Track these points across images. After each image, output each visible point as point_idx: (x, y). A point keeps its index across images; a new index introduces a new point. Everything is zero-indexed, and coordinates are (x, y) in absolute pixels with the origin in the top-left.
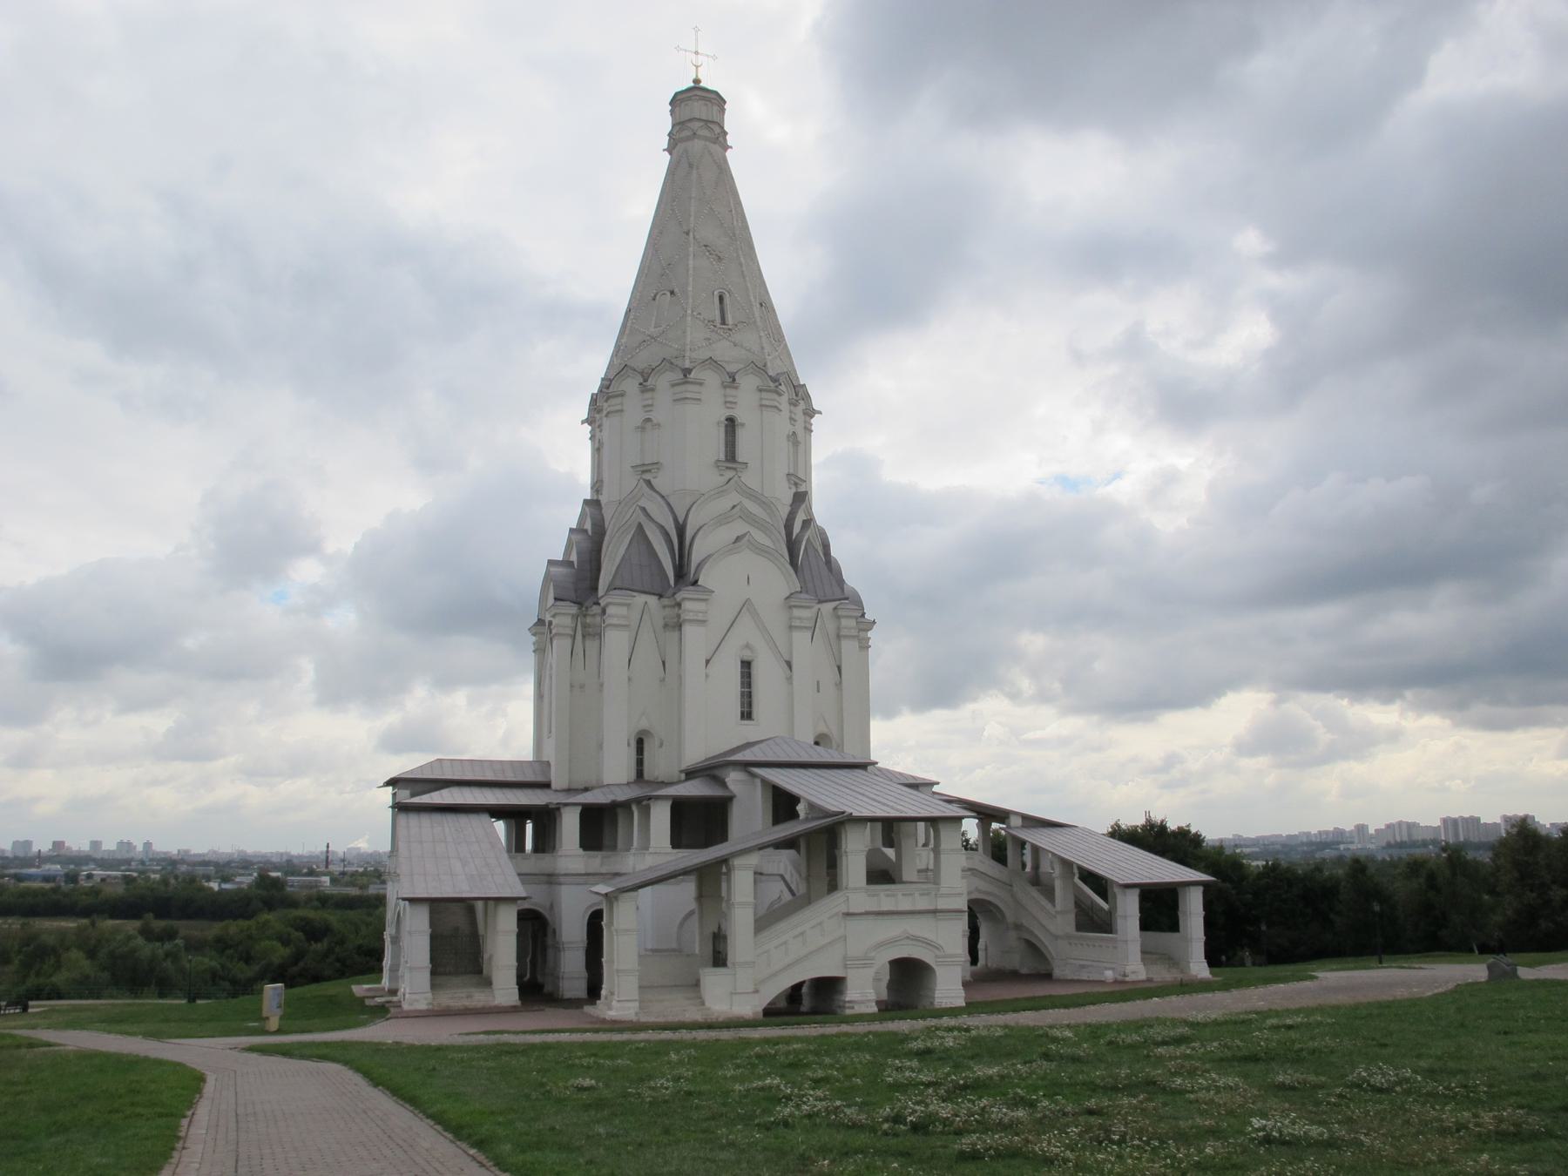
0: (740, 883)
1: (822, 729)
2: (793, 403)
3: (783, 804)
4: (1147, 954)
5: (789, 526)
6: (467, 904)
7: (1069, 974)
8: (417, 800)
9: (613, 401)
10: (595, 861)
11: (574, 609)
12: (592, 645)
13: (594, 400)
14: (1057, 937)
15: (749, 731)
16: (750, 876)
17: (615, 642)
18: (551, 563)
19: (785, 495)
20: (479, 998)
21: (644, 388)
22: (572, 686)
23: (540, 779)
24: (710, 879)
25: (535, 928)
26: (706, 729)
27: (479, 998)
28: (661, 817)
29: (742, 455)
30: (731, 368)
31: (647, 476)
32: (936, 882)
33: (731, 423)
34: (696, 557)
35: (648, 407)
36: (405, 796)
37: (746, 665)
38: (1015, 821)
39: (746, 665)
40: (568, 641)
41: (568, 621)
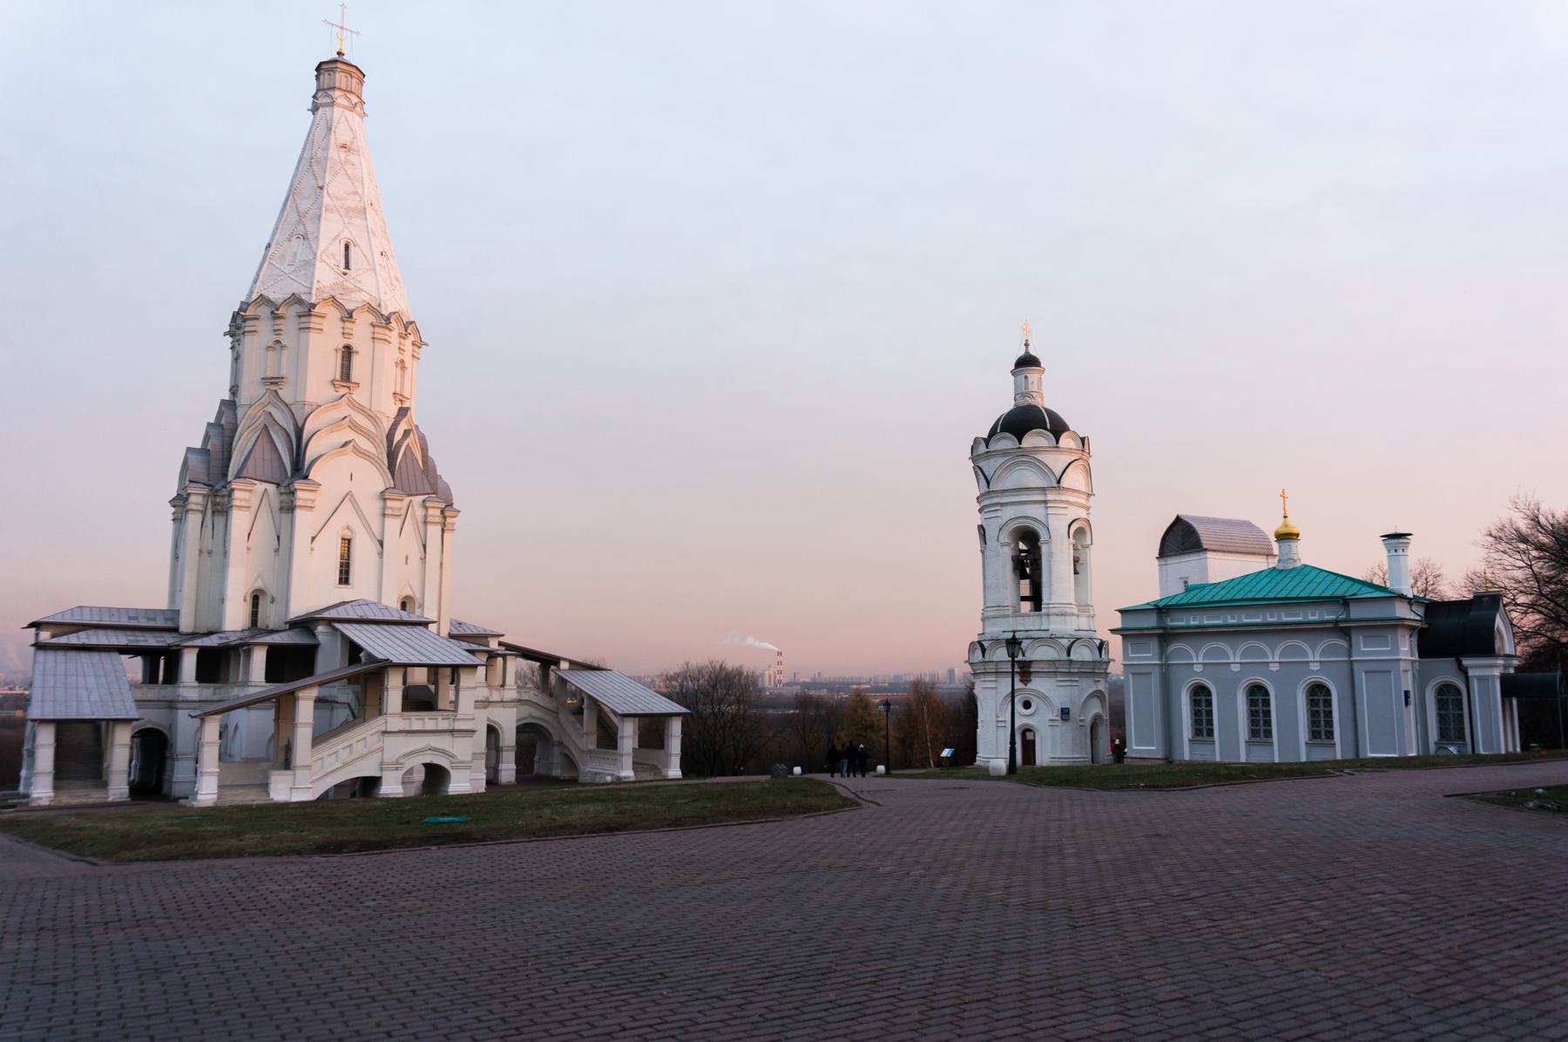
0: (305, 709)
1: (408, 592)
2: (403, 337)
3: (354, 651)
4: (636, 765)
5: (390, 436)
6: (95, 724)
7: (588, 779)
8: (55, 641)
9: (249, 323)
10: (208, 691)
11: (205, 491)
12: (220, 520)
13: (235, 316)
14: (582, 752)
15: (346, 593)
16: (311, 704)
17: (239, 520)
18: (189, 449)
19: (392, 411)
20: (95, 796)
21: (275, 316)
22: (201, 551)
23: (170, 624)
24: (284, 706)
25: (155, 748)
26: (311, 590)
27: (95, 796)
28: (259, 658)
29: (354, 378)
30: (349, 307)
31: (274, 387)
32: (456, 711)
33: (348, 352)
34: (310, 454)
36: (45, 636)
37: (347, 542)
38: (564, 665)
39: (347, 542)
40: (200, 516)
41: (199, 499)
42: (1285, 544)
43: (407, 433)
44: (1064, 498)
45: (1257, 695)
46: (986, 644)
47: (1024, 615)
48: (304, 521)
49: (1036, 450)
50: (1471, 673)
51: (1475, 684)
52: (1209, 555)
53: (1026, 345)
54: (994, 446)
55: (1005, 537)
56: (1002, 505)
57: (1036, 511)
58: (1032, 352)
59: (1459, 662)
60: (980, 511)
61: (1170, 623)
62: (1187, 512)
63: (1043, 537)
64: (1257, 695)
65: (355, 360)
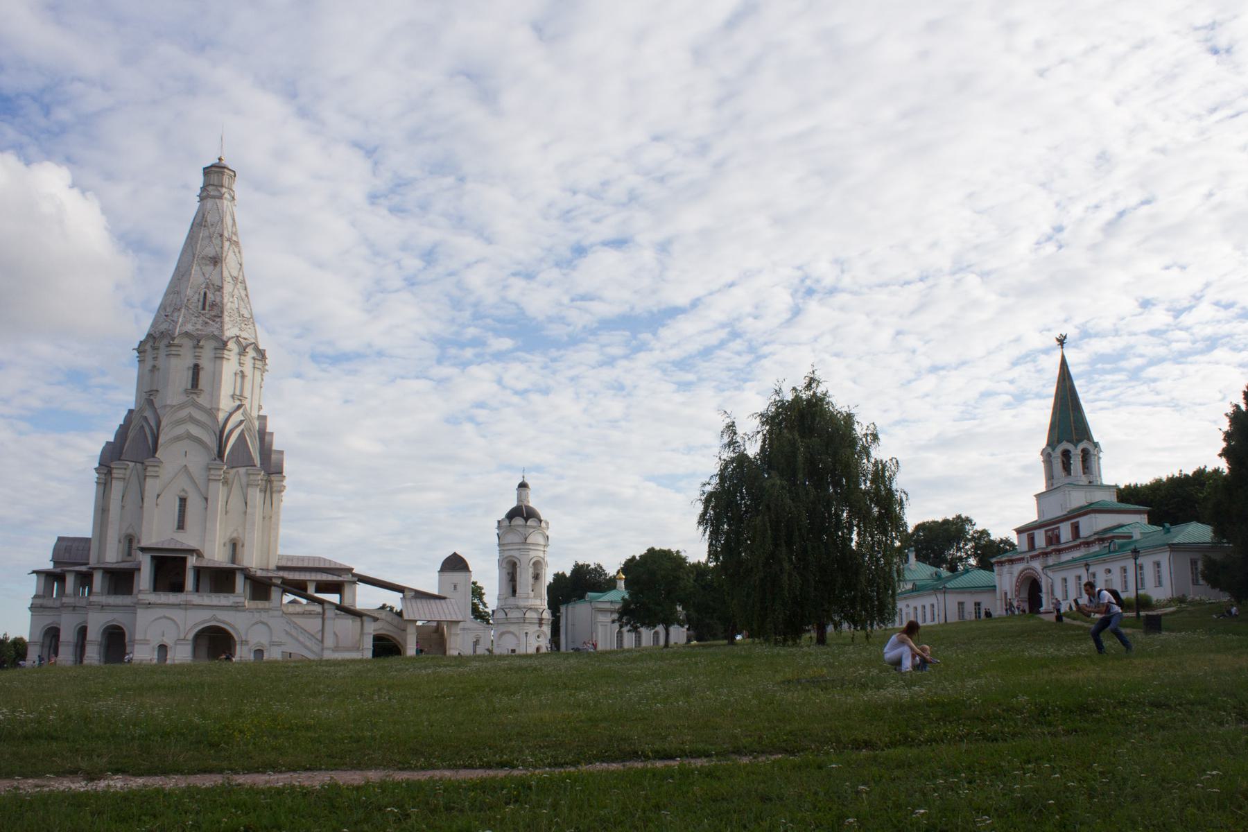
17: (117, 487)
33: (196, 369)
34: (161, 441)
35: (155, 359)
37: (183, 501)
39: (183, 501)
43: (241, 422)
48: (151, 486)
65: (202, 375)
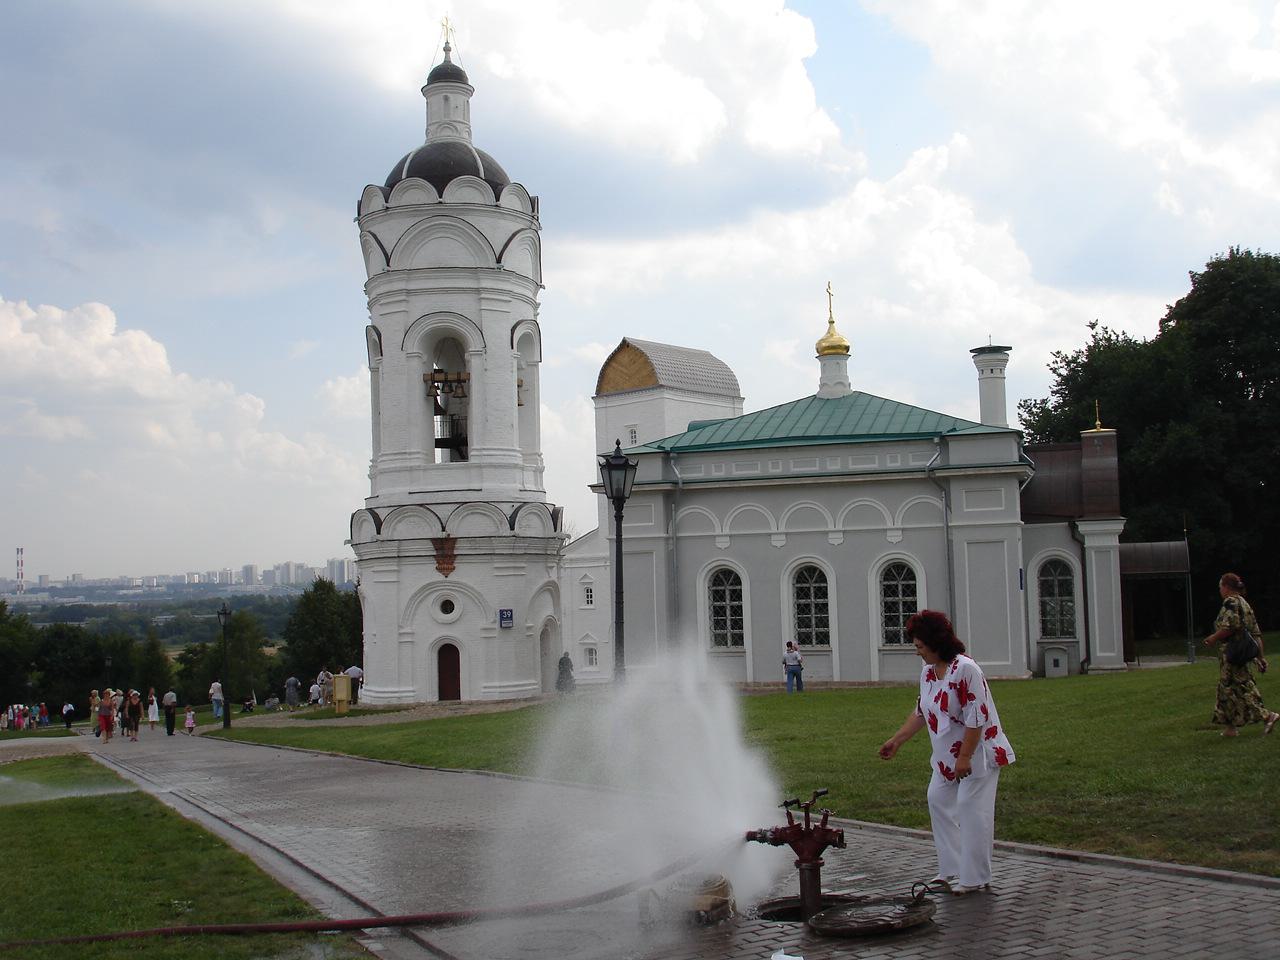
42: (831, 362)
44: (507, 286)
45: (810, 583)
46: (382, 514)
47: (438, 468)
49: (467, 207)
50: (1088, 543)
51: (1092, 558)
52: (667, 394)
53: (447, 49)
54: (399, 198)
55: (414, 345)
56: (409, 292)
57: (463, 305)
58: (455, 61)
59: (1073, 528)
60: (370, 306)
61: (679, 474)
62: (639, 334)
63: (474, 344)
64: (810, 583)
